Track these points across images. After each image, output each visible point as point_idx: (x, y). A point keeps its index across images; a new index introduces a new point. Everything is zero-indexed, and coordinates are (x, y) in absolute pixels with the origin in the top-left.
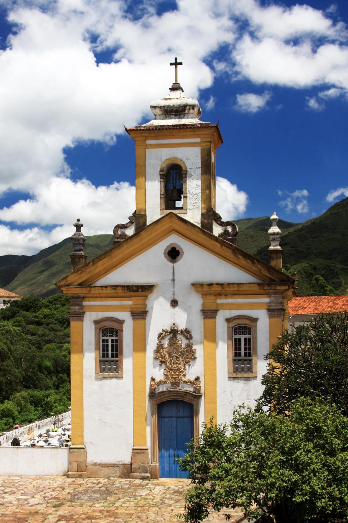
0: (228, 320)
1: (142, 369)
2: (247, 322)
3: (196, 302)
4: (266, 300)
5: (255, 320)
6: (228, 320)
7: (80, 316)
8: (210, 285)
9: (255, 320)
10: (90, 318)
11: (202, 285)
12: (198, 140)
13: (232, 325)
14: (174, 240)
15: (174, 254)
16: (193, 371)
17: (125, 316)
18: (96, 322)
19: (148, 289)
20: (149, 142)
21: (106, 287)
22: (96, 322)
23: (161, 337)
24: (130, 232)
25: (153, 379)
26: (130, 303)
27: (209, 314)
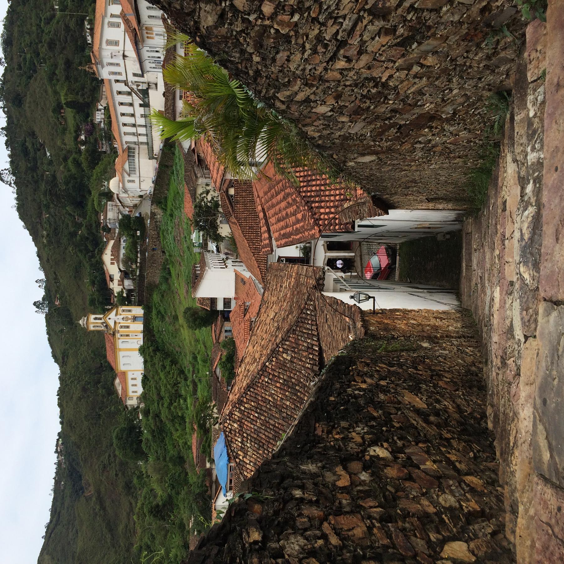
1: (129, 323)
3: (118, 317)
16: (130, 317)
19: (115, 322)
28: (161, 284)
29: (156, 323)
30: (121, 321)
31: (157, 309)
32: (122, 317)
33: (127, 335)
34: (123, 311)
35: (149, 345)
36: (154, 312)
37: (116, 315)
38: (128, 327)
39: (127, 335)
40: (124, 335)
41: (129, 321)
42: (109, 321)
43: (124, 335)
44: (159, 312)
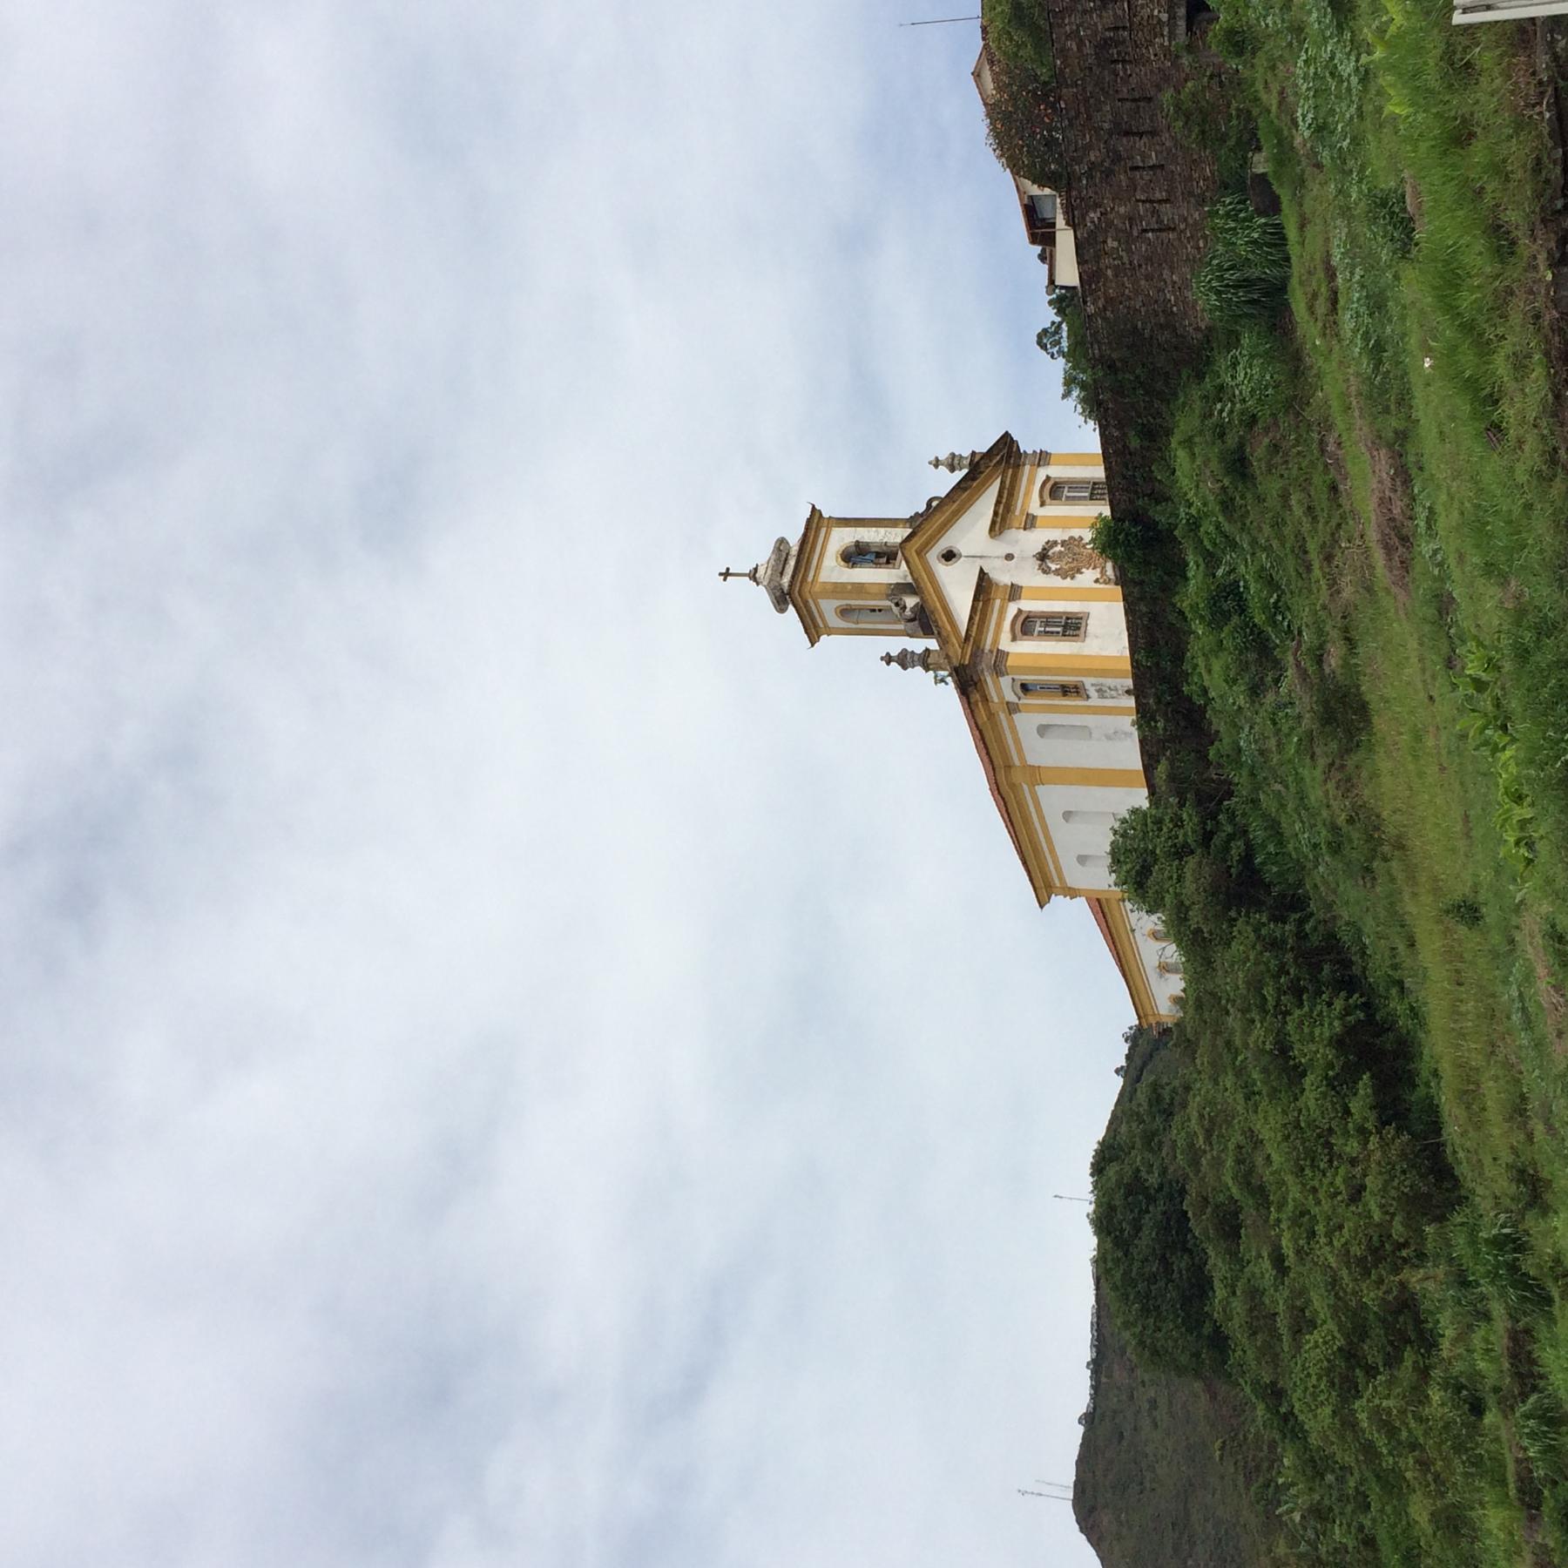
0: (1043, 504)
2: (1048, 486)
4: (1027, 467)
5: (1048, 478)
6: (1043, 504)
7: (1002, 656)
8: (996, 513)
9: (1048, 478)
10: (1005, 644)
11: (993, 523)
12: (823, 530)
13: (1048, 500)
14: (933, 556)
15: (949, 556)
17: (1012, 609)
18: (1014, 639)
20: (810, 579)
21: (971, 618)
22: (1014, 639)
23: (1046, 571)
24: (911, 602)
25: (1097, 581)
26: (998, 602)
27: (1030, 522)
28: (1233, 340)
29: (1213, 672)
30: (1028, 576)
31: (1211, 560)
32: (1034, 540)
33: (1065, 690)
34: (1055, 490)
35: (1189, 832)
36: (1193, 591)
37: (998, 526)
38: (1071, 626)
39: (1065, 690)
40: (1046, 689)
41: (1088, 577)
42: (943, 571)
43: (1046, 689)
44: (1227, 601)
